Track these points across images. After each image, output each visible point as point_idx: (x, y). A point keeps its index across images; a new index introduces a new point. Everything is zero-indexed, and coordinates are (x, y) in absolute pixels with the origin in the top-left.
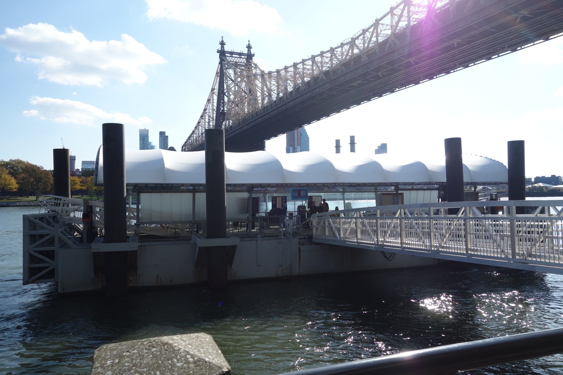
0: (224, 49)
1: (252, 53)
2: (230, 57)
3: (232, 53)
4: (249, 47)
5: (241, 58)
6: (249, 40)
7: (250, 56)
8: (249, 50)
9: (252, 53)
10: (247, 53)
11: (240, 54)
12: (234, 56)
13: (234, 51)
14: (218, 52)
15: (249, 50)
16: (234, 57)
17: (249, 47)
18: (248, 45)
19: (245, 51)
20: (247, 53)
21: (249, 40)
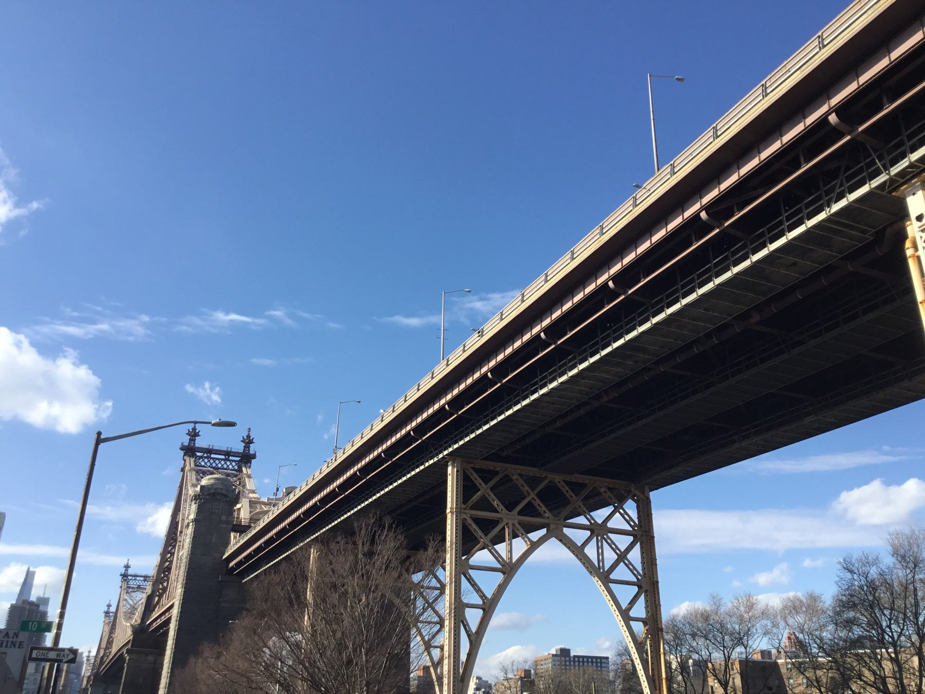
0: (194, 444)
4: (248, 441)
6: (250, 428)
9: (252, 452)
11: (228, 454)
12: (213, 456)
14: (181, 449)
17: (248, 441)
19: (239, 447)
21: (250, 428)
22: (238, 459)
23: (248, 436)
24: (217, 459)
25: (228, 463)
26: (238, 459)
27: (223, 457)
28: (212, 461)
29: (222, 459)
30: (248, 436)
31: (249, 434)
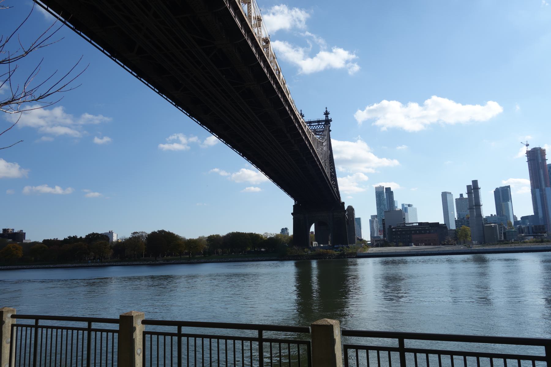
1: (329, 119)
2: (310, 125)
3: (310, 123)
4: (327, 114)
5: (319, 125)
7: (328, 122)
8: (327, 117)
9: (329, 118)
10: (325, 119)
11: (319, 122)
12: (312, 124)
13: (311, 121)
15: (327, 117)
16: (312, 125)
17: (327, 114)
18: (325, 112)
19: (323, 118)
20: (325, 119)
22: (323, 123)
23: (326, 111)
24: (314, 125)
25: (320, 126)
26: (323, 123)
27: (317, 124)
28: (312, 127)
29: (316, 125)
30: (326, 111)
31: (326, 110)
